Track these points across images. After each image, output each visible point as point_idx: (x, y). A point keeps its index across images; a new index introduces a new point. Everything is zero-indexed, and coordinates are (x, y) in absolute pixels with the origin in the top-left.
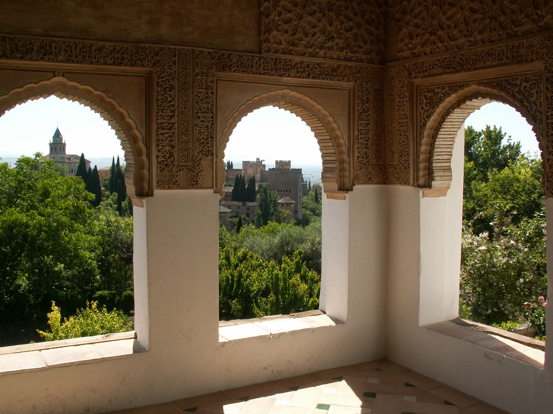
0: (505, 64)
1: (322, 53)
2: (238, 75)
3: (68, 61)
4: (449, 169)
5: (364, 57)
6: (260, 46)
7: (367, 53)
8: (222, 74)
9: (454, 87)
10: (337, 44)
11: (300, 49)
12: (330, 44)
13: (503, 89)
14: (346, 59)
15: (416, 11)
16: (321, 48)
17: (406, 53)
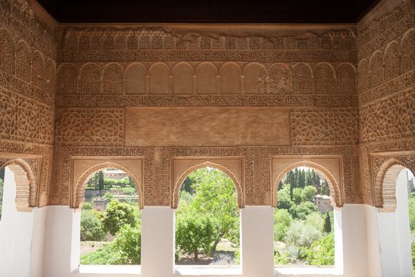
0: (402, 150)
1: (323, 142)
2: (281, 156)
3: (211, 155)
4: (395, 198)
5: (346, 142)
6: (291, 142)
7: (349, 139)
8: (274, 156)
9: (386, 158)
10: (331, 138)
11: (312, 141)
12: (327, 138)
13: (404, 162)
14: (336, 144)
15: (369, 119)
16: (322, 140)
17: (366, 140)
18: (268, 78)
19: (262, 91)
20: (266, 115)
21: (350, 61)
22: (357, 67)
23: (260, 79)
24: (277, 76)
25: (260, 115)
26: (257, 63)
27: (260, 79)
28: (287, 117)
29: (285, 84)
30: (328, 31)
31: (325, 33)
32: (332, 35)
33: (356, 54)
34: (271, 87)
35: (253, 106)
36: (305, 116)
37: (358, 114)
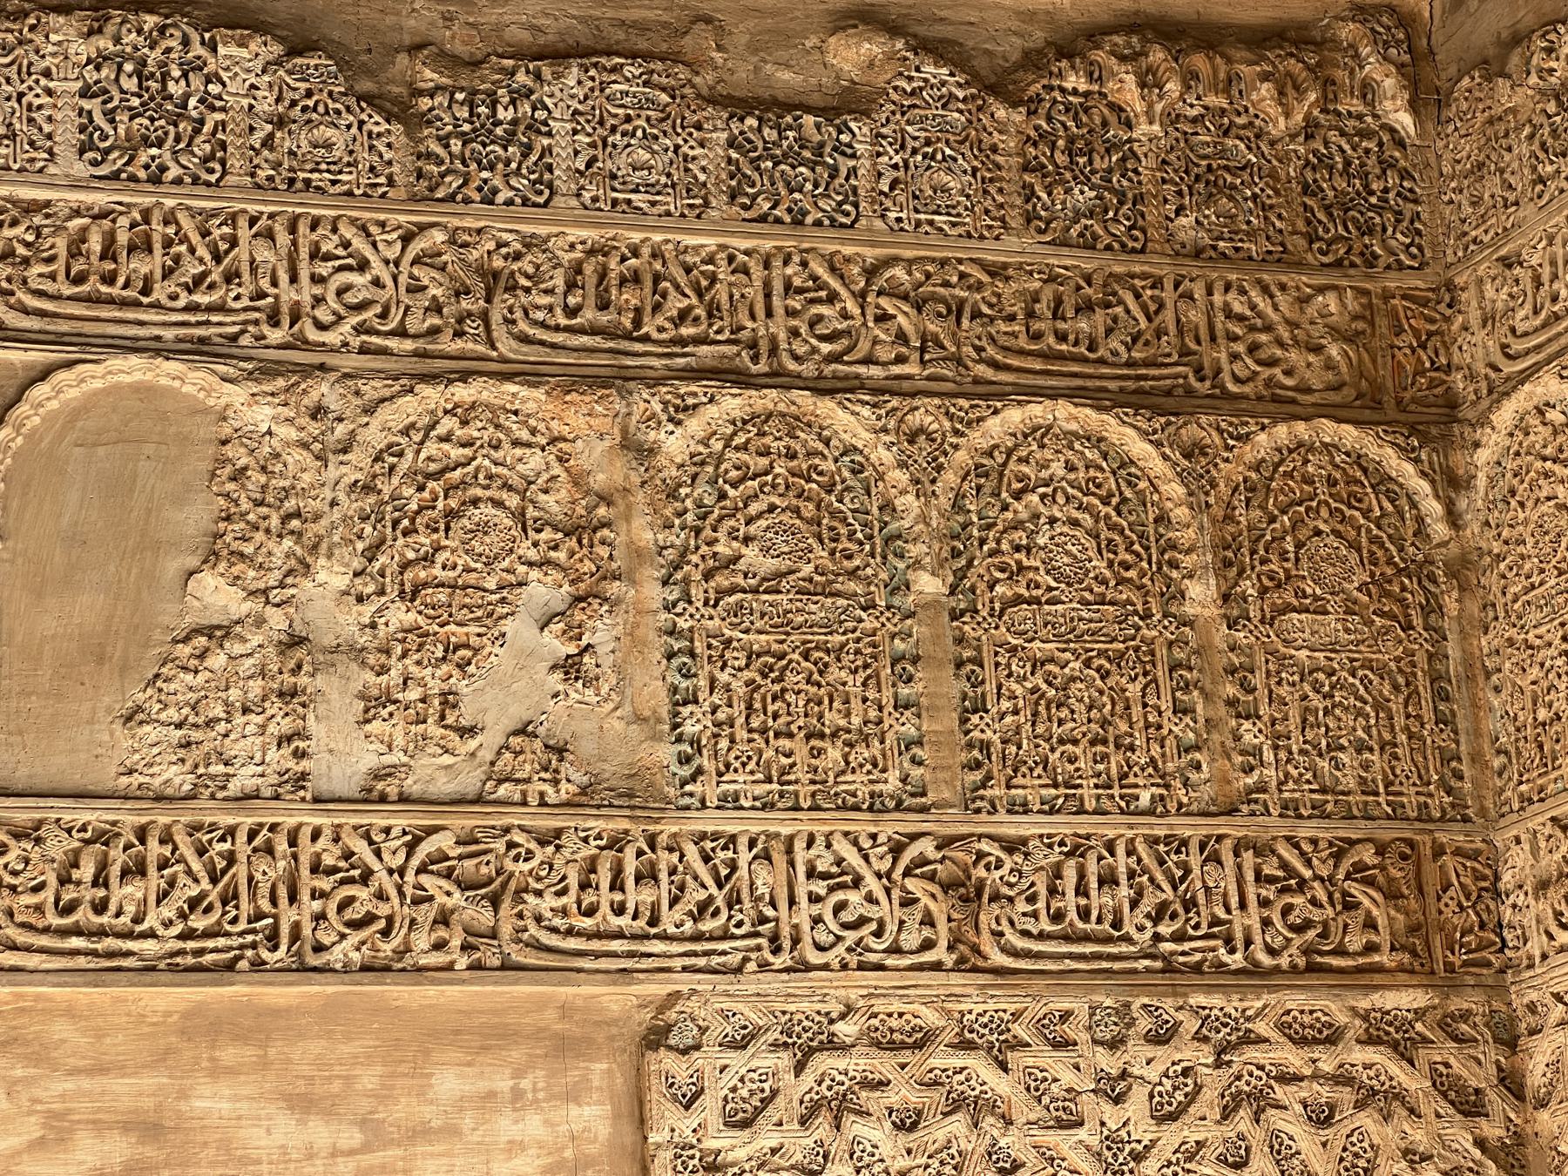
18: (332, 576)
19: (252, 756)
20: (303, 1104)
21: (1364, 404)
22: (1451, 483)
23: (217, 595)
24: (454, 557)
25: (211, 1101)
26: (190, 380)
27: (217, 595)
28: (593, 1118)
29: (570, 667)
30: (1094, 34)
31: (1066, 52)
32: (1149, 81)
33: (1434, 338)
34: (375, 704)
35: (111, 967)
36: (838, 1106)
37: (1512, 1083)
